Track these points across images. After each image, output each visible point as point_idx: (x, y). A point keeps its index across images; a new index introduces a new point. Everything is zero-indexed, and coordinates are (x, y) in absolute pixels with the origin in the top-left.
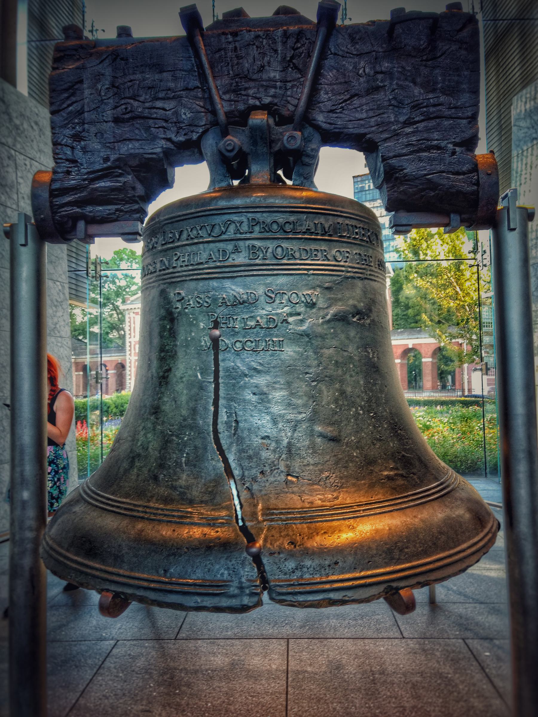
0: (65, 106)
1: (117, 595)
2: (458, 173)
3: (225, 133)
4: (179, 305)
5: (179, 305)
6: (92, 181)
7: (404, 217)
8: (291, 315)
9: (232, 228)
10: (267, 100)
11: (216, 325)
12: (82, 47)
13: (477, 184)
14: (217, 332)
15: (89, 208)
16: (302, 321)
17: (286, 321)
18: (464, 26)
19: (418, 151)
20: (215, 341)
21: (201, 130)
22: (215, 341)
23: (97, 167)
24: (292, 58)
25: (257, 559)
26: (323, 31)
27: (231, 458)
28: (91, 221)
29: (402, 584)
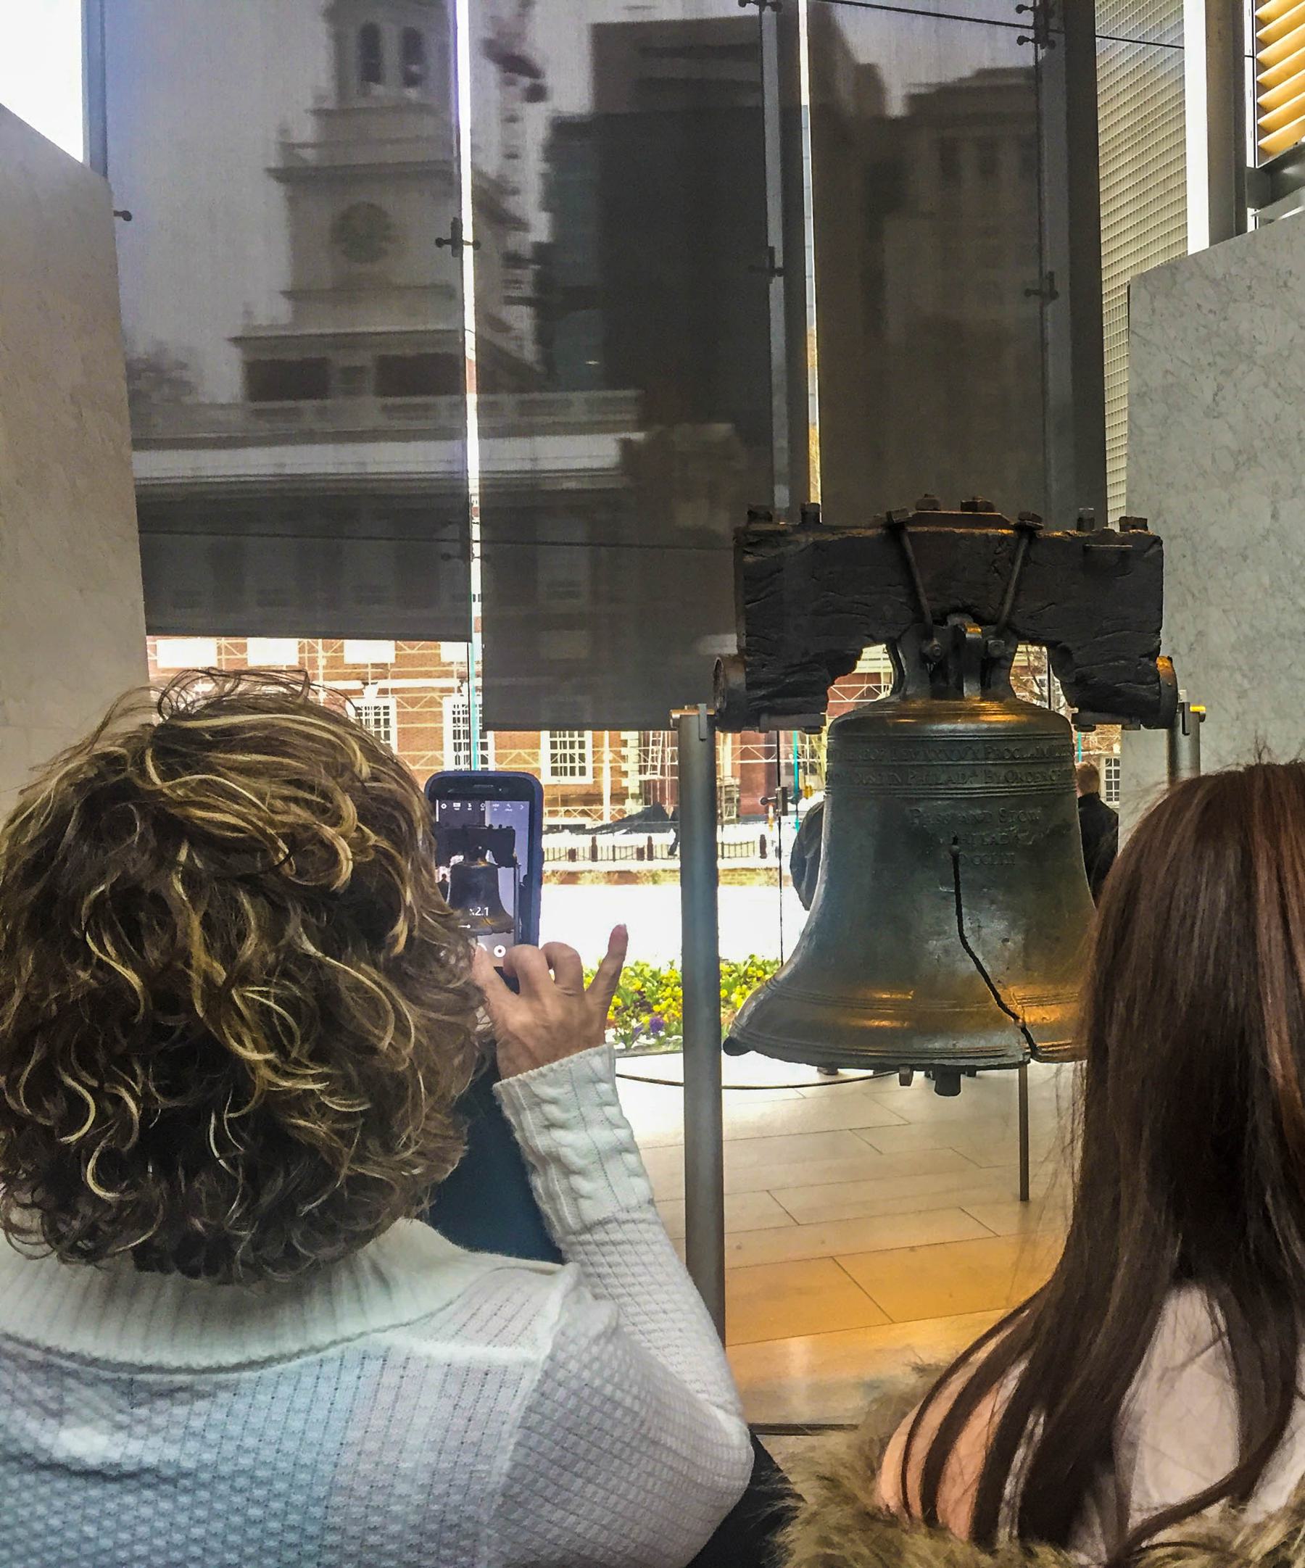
0: (762, 595)
2: (1143, 683)
4: (917, 821)
5: (917, 821)
6: (787, 675)
7: (1089, 715)
8: (1020, 832)
9: (970, 755)
10: (969, 602)
11: (955, 841)
13: (1159, 693)
14: (956, 847)
15: (779, 701)
16: (1028, 838)
18: (1151, 546)
19: (1109, 661)
21: (904, 627)
23: (795, 661)
24: (994, 562)
26: (1025, 541)
28: (773, 712)
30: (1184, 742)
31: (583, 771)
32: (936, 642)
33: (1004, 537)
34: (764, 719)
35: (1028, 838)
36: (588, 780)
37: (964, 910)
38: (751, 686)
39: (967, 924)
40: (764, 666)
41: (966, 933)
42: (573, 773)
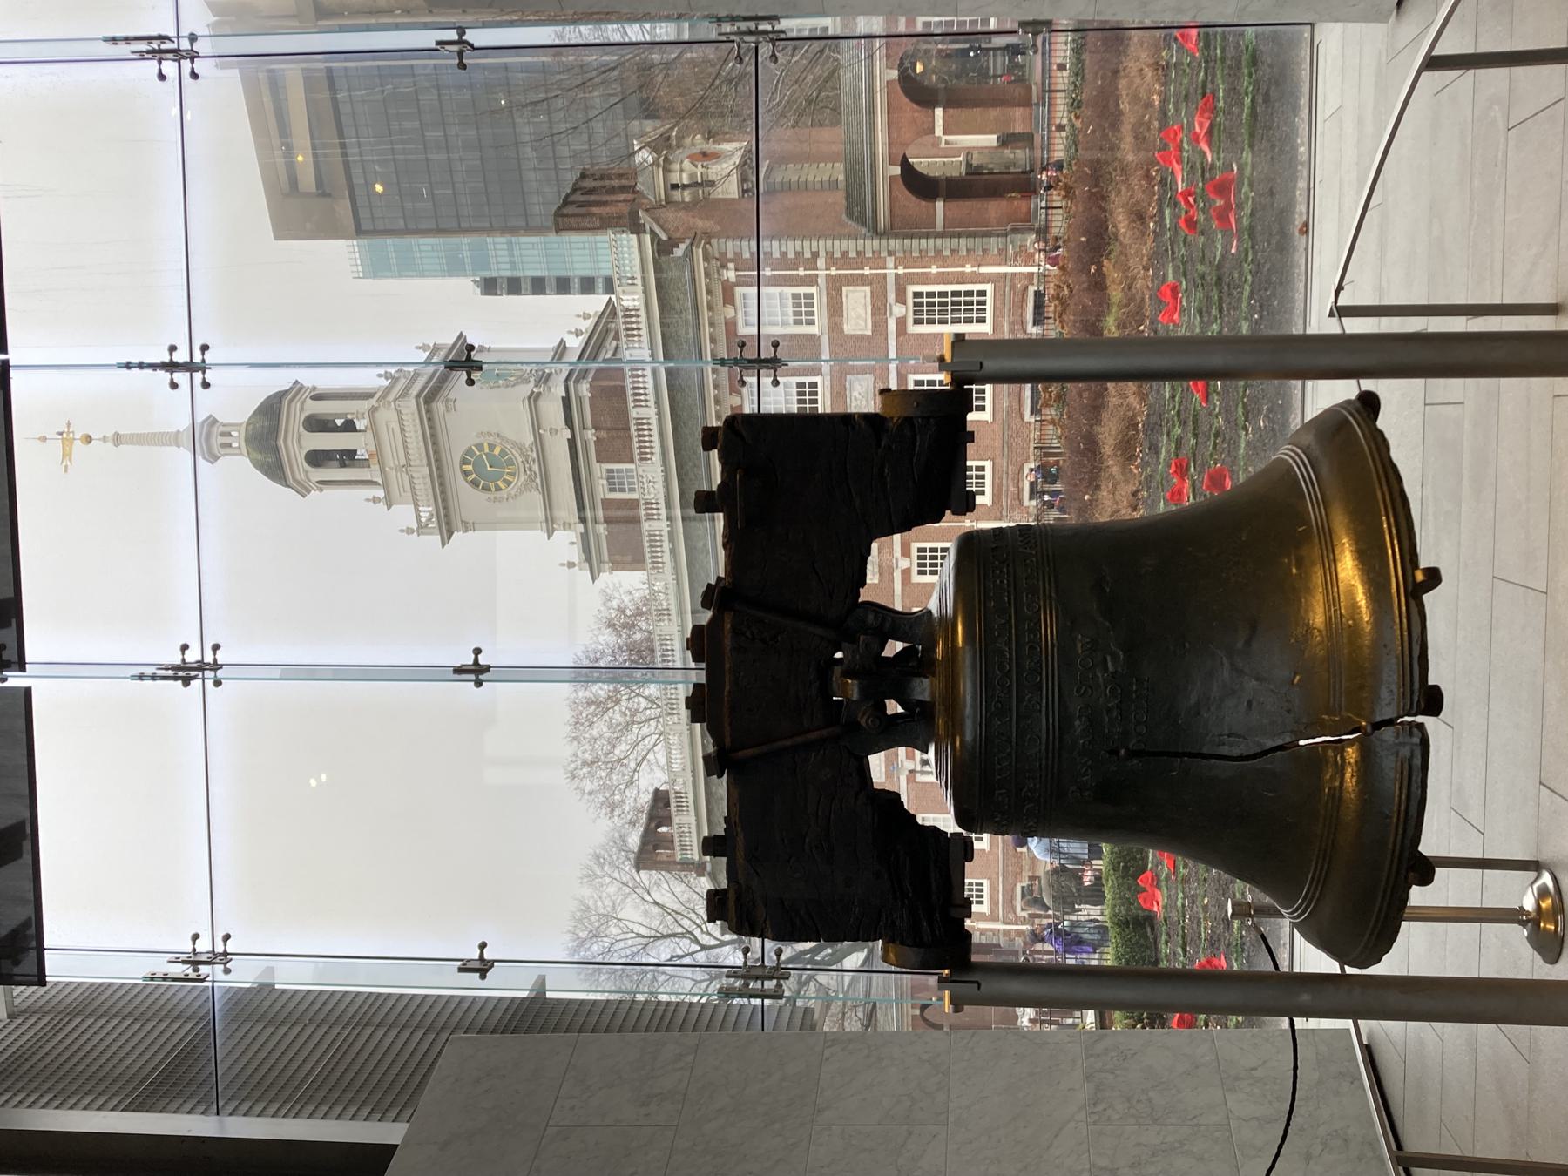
1: (1411, 868)
3: (854, 726)
8: (1106, 669)
11: (1115, 752)
12: (738, 899)
13: (928, 418)
17: (1114, 674)
20: (1133, 754)
22: (1133, 754)
25: (1377, 726)
27: (1270, 744)
29: (1410, 579)
30: (991, 365)
31: (982, 293)
32: (863, 722)
33: (736, 632)
34: (954, 913)
35: (1115, 657)
36: (989, 288)
37: (1205, 750)
38: (917, 942)
39: (1225, 750)
40: (893, 923)
41: (1236, 752)
42: (984, 303)
